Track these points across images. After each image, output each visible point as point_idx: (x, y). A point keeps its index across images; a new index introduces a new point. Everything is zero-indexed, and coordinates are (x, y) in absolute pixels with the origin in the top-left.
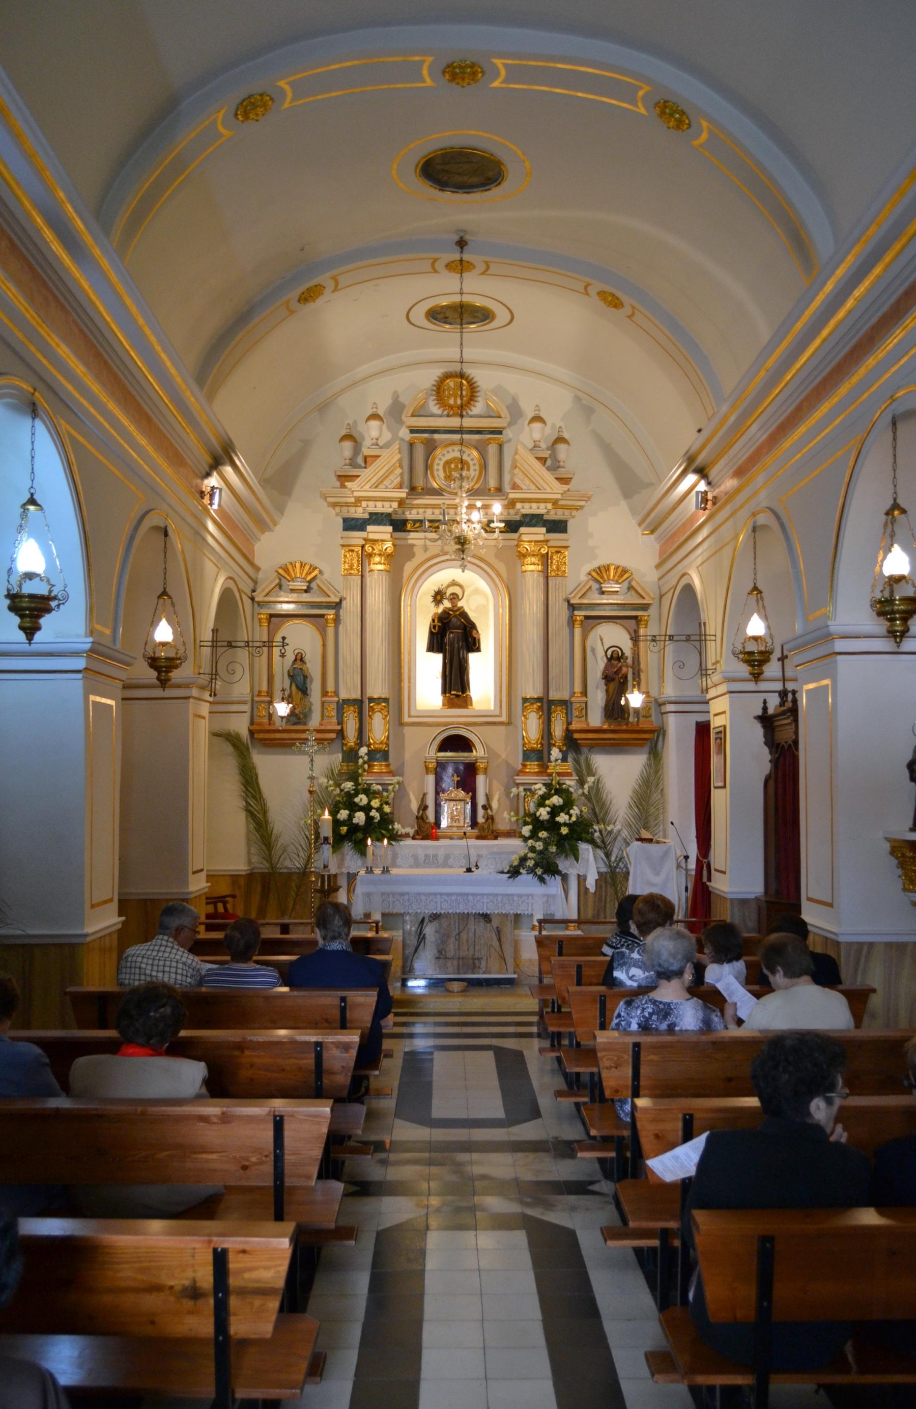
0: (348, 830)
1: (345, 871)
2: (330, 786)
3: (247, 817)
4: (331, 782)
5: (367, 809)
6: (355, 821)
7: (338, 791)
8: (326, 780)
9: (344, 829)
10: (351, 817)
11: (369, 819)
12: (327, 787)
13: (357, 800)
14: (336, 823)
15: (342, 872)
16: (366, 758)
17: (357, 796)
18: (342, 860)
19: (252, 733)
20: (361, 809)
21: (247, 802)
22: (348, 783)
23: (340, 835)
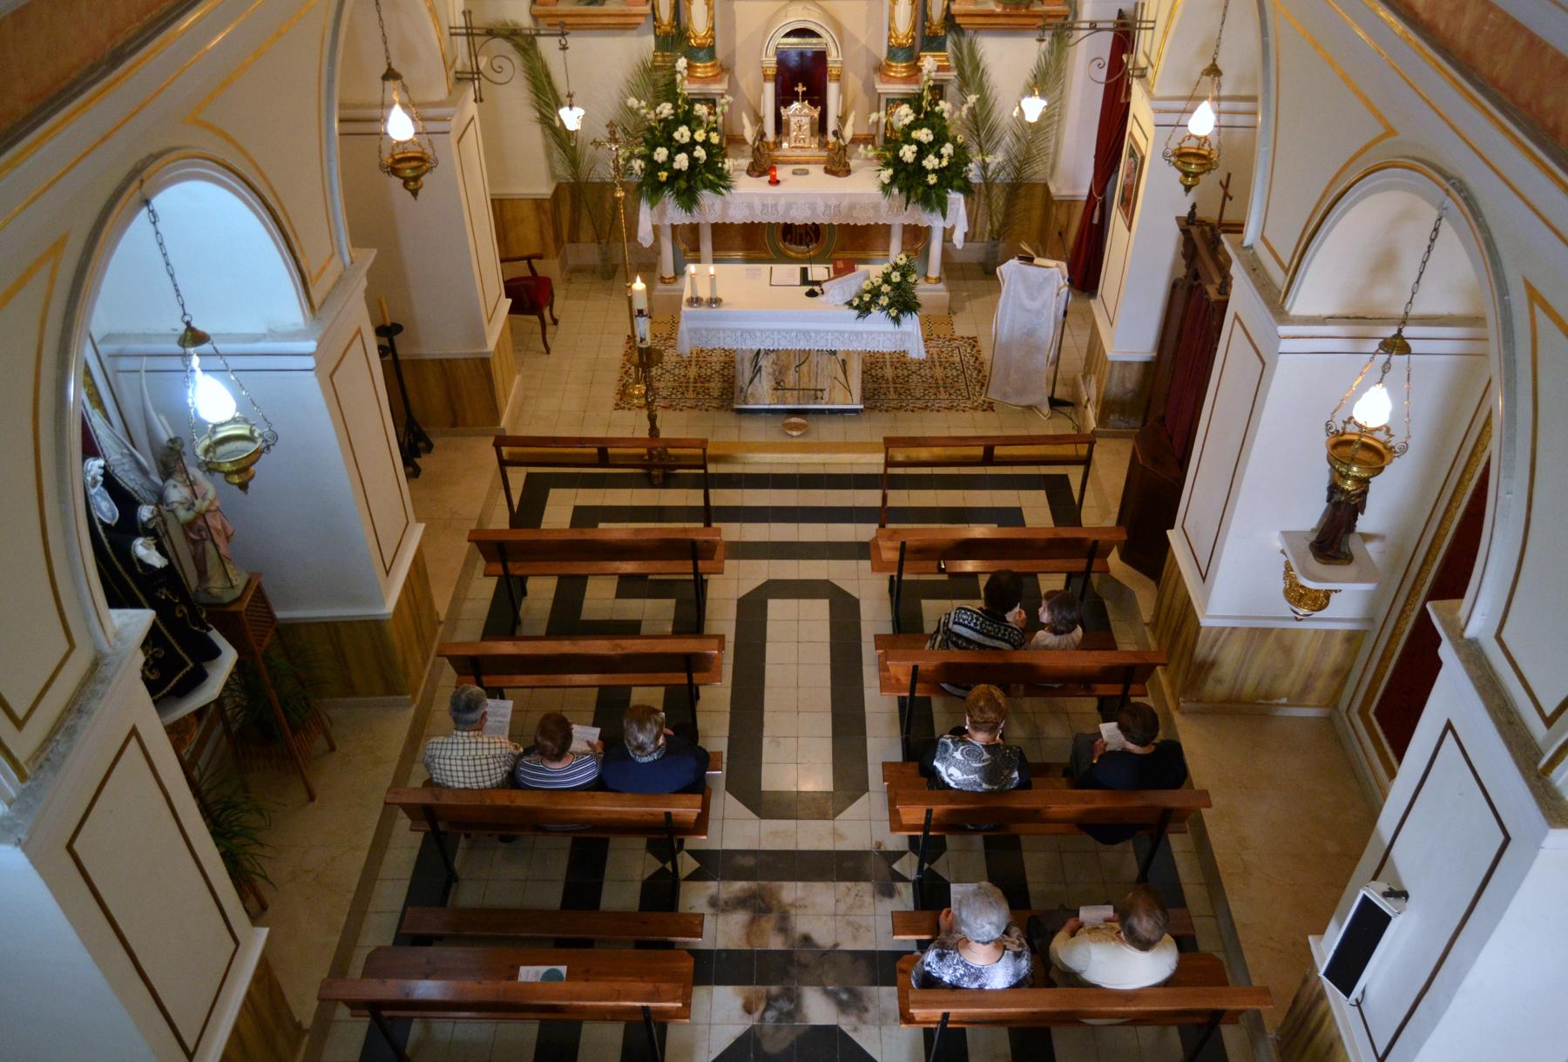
0: (668, 178)
1: (667, 222)
2: (643, 108)
3: (543, 130)
4: (643, 103)
5: (689, 148)
6: (676, 166)
7: (651, 116)
8: (637, 102)
9: (663, 175)
10: (671, 159)
11: (693, 161)
12: (638, 109)
13: (677, 135)
14: (653, 167)
15: (665, 226)
16: (685, 73)
17: (676, 130)
18: (663, 213)
19: (535, 17)
20: (682, 148)
21: (541, 113)
22: (664, 104)
23: (659, 182)
